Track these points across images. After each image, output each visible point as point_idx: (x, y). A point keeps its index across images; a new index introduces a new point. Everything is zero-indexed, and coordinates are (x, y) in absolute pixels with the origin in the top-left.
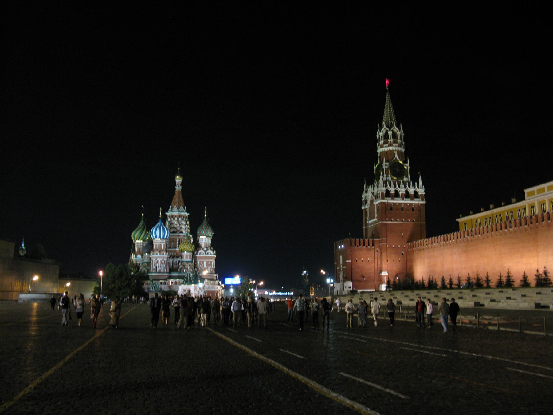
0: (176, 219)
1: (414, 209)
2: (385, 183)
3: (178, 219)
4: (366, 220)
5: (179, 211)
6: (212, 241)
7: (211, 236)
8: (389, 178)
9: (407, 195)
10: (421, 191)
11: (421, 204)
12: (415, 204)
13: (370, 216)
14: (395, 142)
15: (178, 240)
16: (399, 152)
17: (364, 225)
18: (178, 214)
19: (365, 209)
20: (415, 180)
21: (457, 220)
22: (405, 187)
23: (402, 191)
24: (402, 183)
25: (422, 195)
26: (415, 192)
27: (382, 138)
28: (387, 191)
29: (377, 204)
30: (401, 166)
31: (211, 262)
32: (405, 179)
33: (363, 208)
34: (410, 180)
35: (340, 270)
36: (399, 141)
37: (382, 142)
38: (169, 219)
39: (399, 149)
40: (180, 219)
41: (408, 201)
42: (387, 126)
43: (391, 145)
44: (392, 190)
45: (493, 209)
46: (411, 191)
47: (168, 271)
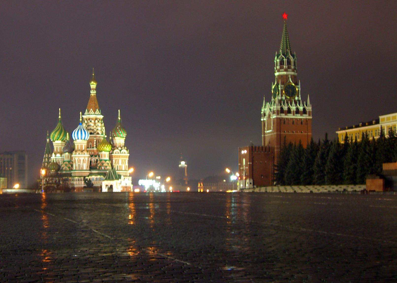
0: (93, 121)
1: (303, 123)
2: (280, 101)
4: (264, 130)
6: (125, 141)
7: (125, 136)
8: (284, 98)
9: (297, 111)
10: (309, 108)
11: (309, 119)
12: (304, 119)
13: (267, 128)
14: (289, 68)
15: (95, 141)
16: (292, 76)
17: (263, 133)
18: (93, 117)
19: (264, 121)
20: (304, 99)
21: (337, 132)
22: (296, 105)
23: (293, 108)
24: (293, 102)
25: (309, 112)
26: (304, 109)
27: (278, 64)
28: (282, 108)
29: (273, 119)
30: (294, 88)
31: (125, 160)
32: (296, 98)
33: (262, 120)
34: (300, 99)
35: (243, 170)
36: (293, 67)
37: (278, 67)
38: (86, 122)
39: (293, 73)
40: (96, 121)
41: (298, 116)
42: (283, 54)
43: (286, 70)
44: (285, 108)
45: (361, 127)
46: (301, 108)
47: (89, 169)
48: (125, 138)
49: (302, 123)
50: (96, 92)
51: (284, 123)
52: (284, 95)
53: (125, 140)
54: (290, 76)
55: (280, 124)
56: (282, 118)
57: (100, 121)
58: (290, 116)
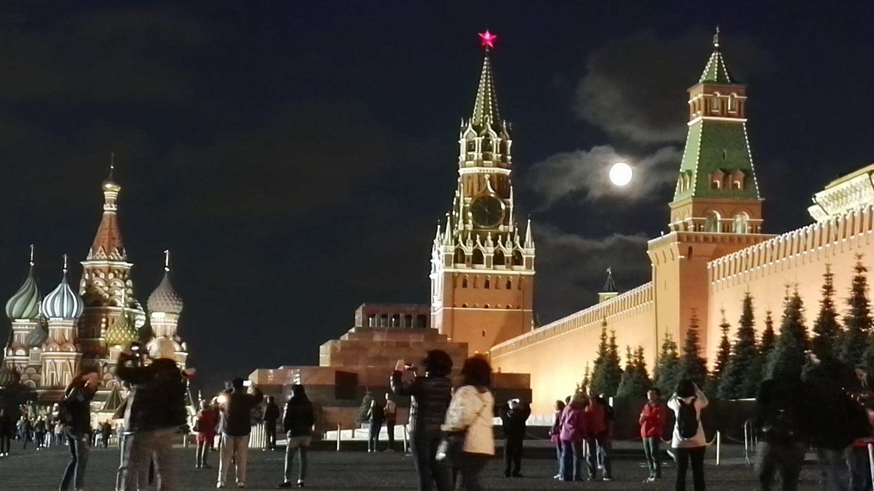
0: (102, 276)
3: (106, 276)
5: (109, 260)
7: (179, 312)
8: (470, 227)
10: (529, 251)
14: (486, 157)
18: (106, 267)
23: (488, 251)
30: (493, 204)
36: (495, 156)
38: (87, 276)
40: (111, 276)
41: (502, 270)
43: (479, 164)
44: (469, 250)
46: (508, 252)
48: (178, 316)
49: (509, 285)
50: (118, 207)
51: (465, 285)
52: (470, 221)
53: (179, 320)
54: (487, 177)
55: (455, 286)
56: (459, 273)
57: (121, 276)
58: (481, 269)
